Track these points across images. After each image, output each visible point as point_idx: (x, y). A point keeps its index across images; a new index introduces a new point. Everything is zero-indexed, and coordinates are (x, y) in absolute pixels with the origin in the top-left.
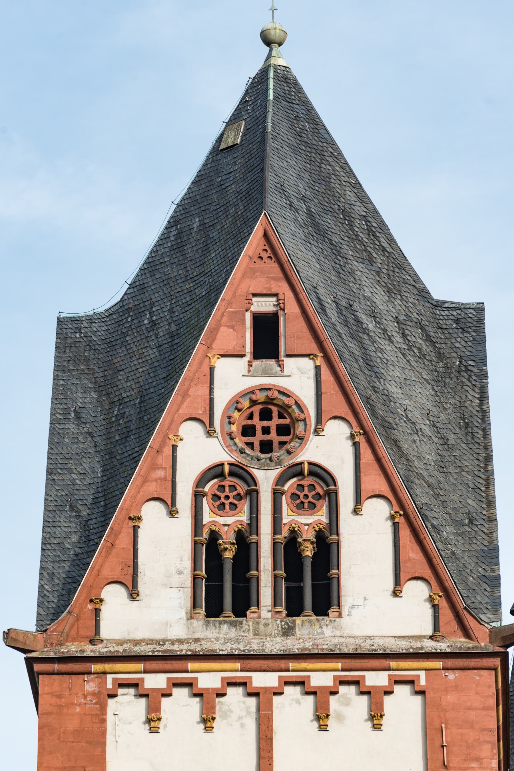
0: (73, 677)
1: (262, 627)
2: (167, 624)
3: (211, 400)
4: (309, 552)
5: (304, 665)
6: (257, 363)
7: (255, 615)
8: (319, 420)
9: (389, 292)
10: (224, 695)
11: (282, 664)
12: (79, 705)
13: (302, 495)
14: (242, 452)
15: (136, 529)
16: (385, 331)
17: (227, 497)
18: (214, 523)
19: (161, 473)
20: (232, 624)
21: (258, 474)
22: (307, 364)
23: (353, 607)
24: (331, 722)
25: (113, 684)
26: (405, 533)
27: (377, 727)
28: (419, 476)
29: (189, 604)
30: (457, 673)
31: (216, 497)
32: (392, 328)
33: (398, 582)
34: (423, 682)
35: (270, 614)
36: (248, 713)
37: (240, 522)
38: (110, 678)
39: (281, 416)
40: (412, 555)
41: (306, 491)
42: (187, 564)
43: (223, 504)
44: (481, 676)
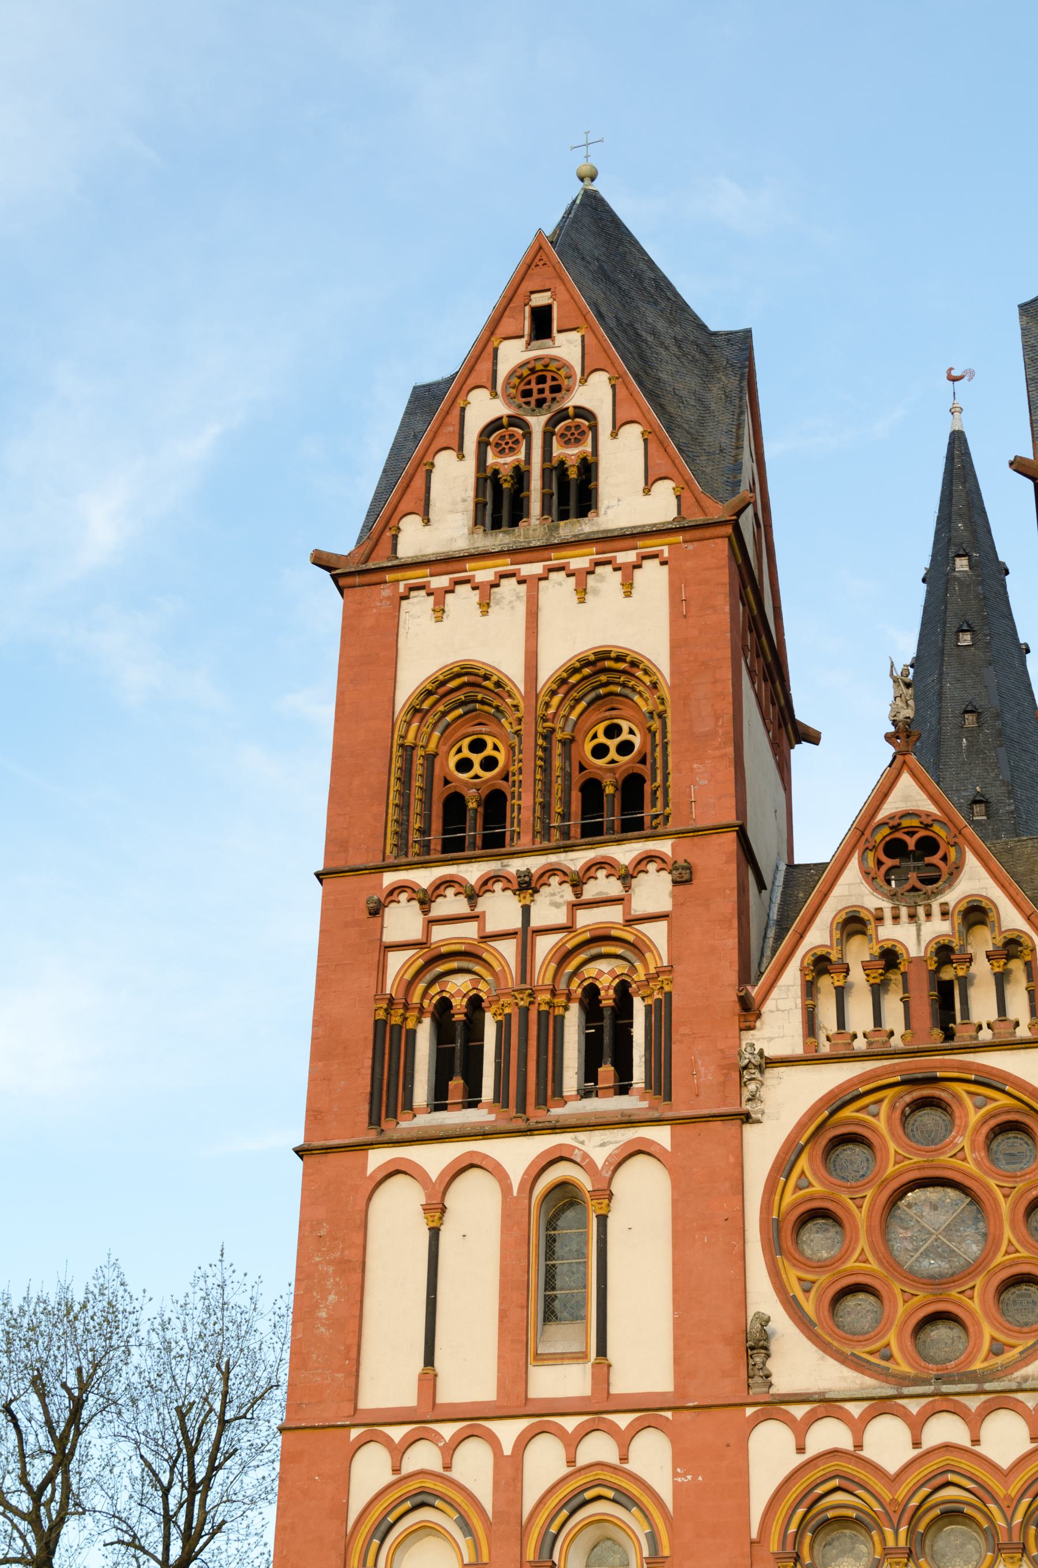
0: (372, 587)
1: (531, 532)
2: (452, 539)
3: (495, 372)
4: (573, 474)
5: (564, 553)
6: (535, 343)
7: (526, 524)
8: (583, 373)
9: (670, 322)
10: (497, 585)
11: (545, 554)
12: (376, 607)
13: (569, 437)
14: (520, 407)
15: (429, 473)
16: (662, 344)
17: (507, 443)
18: (496, 463)
19: (450, 429)
20: (505, 532)
21: (531, 420)
22: (575, 336)
23: (608, 508)
24: (589, 597)
25: (405, 588)
26: (652, 446)
27: (628, 594)
28: (679, 426)
29: (471, 522)
30: (695, 544)
31: (497, 445)
32: (669, 342)
33: (646, 483)
34: (666, 554)
35: (538, 522)
36: (518, 598)
37: (518, 460)
38: (402, 585)
39: (554, 379)
40: (658, 461)
41: (573, 430)
42: (471, 493)
43: (504, 449)
44: (716, 544)
